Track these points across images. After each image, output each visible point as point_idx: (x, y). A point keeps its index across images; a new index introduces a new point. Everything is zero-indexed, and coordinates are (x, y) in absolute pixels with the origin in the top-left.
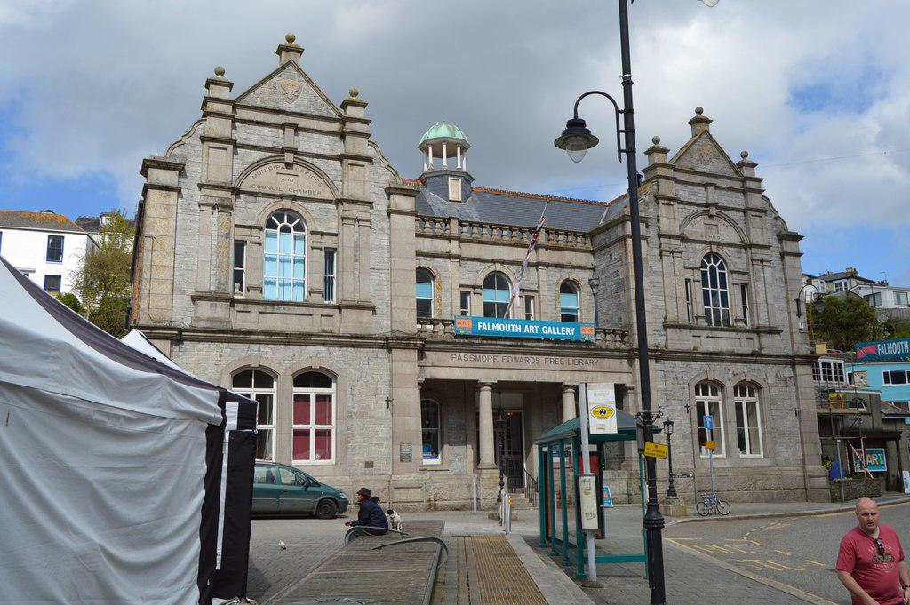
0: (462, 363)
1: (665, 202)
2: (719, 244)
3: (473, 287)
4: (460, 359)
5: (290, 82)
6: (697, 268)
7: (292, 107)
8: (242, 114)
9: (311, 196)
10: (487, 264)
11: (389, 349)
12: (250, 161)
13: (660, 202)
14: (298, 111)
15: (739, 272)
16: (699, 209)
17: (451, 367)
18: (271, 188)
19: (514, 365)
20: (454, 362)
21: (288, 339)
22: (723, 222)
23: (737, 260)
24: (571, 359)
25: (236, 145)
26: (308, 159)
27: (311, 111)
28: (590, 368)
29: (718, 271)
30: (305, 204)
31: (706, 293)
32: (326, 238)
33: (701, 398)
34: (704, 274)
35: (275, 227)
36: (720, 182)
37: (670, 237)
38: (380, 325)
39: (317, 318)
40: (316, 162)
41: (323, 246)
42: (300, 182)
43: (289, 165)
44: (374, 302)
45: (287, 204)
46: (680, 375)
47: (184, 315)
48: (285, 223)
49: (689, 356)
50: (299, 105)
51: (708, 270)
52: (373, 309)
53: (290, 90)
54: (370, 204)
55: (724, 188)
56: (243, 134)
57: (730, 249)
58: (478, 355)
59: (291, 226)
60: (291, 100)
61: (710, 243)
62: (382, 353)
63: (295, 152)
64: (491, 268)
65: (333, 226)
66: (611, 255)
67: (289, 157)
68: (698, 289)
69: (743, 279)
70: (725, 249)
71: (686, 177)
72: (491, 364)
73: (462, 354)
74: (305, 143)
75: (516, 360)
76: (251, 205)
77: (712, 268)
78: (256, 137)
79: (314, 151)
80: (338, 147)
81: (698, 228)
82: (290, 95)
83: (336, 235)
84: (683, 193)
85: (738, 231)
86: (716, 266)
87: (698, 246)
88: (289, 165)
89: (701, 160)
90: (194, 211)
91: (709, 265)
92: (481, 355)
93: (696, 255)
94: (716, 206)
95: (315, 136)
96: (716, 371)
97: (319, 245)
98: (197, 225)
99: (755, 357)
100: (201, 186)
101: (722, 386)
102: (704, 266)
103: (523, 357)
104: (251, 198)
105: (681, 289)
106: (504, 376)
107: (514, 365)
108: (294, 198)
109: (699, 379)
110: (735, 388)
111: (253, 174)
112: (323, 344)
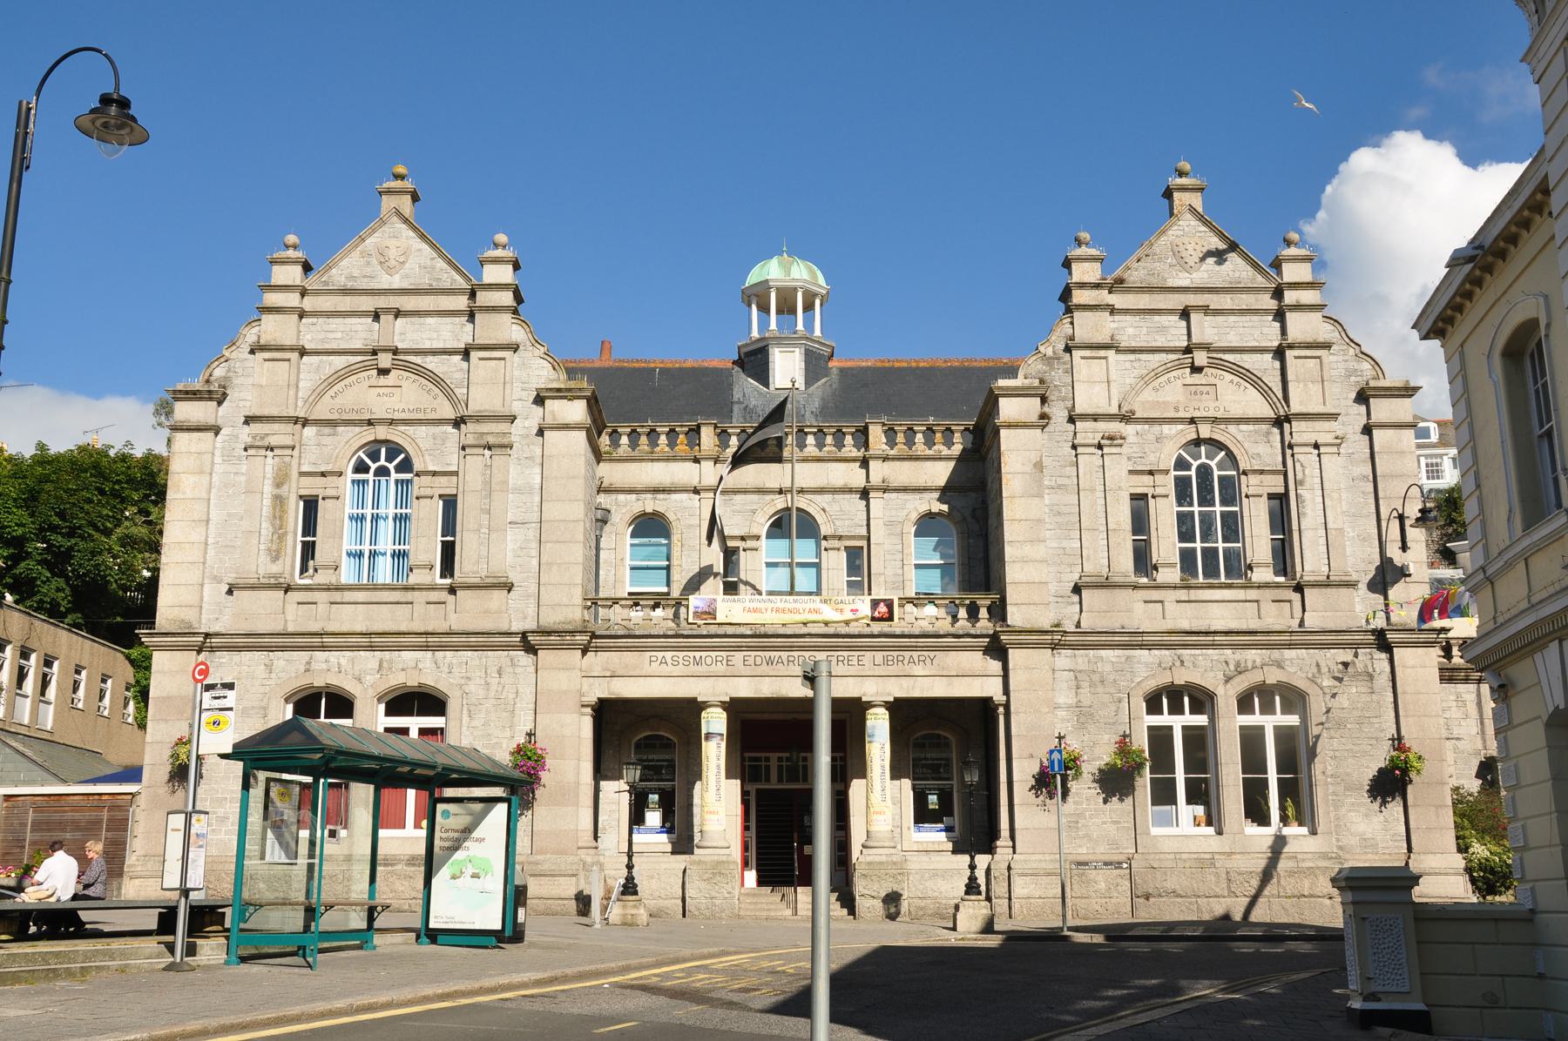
1: (1087, 353)
2: (1215, 421)
3: (743, 538)
4: (664, 662)
5: (392, 243)
6: (1167, 472)
7: (397, 282)
8: (309, 303)
10: (768, 497)
11: (531, 649)
12: (328, 371)
14: (405, 285)
15: (1262, 472)
16: (1163, 357)
17: (651, 678)
18: (418, 410)
19: (764, 669)
21: (373, 641)
22: (1229, 377)
23: (1262, 449)
24: (879, 656)
25: (303, 352)
26: (417, 360)
27: (425, 282)
29: (1216, 473)
30: (410, 430)
31: (1184, 520)
32: (443, 480)
33: (1164, 719)
34: (1182, 487)
35: (366, 470)
37: (1095, 418)
38: (517, 614)
39: (419, 608)
40: (431, 363)
41: (437, 492)
42: (404, 396)
43: (384, 372)
44: (513, 577)
45: (382, 432)
46: (1111, 678)
47: (220, 616)
49: (1135, 641)
50: (407, 276)
51: (1193, 473)
52: (509, 587)
53: (393, 254)
54: (513, 418)
55: (1232, 312)
56: (311, 332)
57: (1243, 427)
58: (698, 654)
59: (391, 466)
60: (390, 271)
61: (1192, 421)
62: (522, 657)
63: (395, 351)
64: (780, 503)
65: (452, 461)
67: (385, 360)
68: (1164, 514)
69: (1275, 484)
70: (1232, 428)
71: (1144, 301)
72: (721, 668)
73: (668, 655)
74: (405, 333)
75: (770, 662)
76: (326, 440)
77: (1204, 472)
78: (339, 335)
79: (427, 345)
80: (461, 333)
81: (1174, 393)
82: (392, 263)
83: (456, 473)
84: (1130, 330)
85: (1265, 391)
87: (1166, 429)
88: (384, 372)
89: (1182, 264)
90: (239, 458)
91: (1195, 464)
92: (704, 654)
93: (1168, 446)
94: (1207, 347)
95: (429, 320)
96: (1202, 668)
97: (428, 492)
98: (243, 478)
99: (1301, 638)
100: (248, 420)
102: (1181, 464)
103: (784, 655)
104: (327, 430)
105: (1122, 515)
106: (745, 689)
107: (764, 669)
108: (392, 422)
111: (331, 392)
112: (426, 648)
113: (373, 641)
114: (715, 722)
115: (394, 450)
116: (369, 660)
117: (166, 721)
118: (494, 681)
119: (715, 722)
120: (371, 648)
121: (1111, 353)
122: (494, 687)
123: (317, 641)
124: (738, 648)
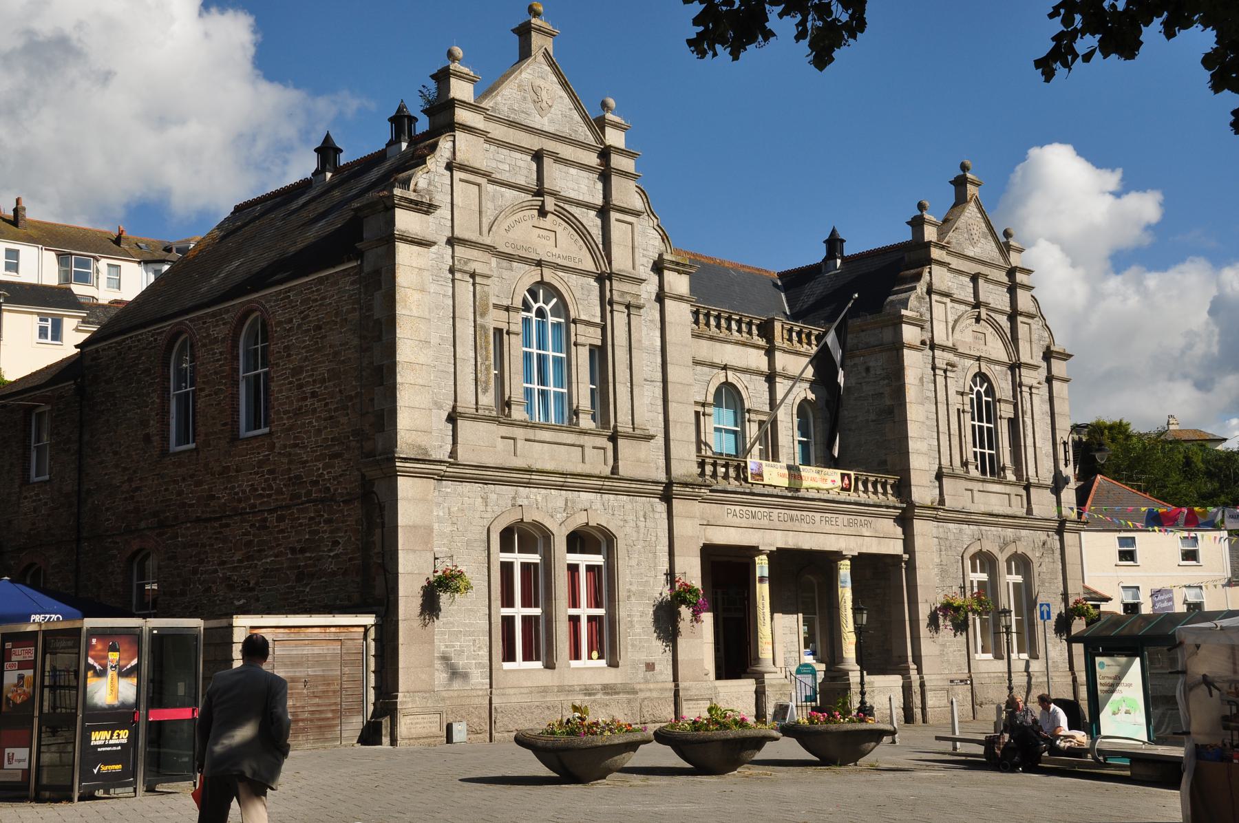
0: (737, 521)
9: (571, 264)
13: (934, 297)
19: (789, 525)
20: (730, 519)
21: (565, 481)
28: (865, 532)
36: (566, 151)
48: (541, 304)
66: (868, 370)
72: (765, 522)
86: (982, 391)
95: (573, 171)
101: (547, 535)
104: (505, 263)
107: (789, 525)
109: (972, 550)
110: (1008, 561)
113: (565, 481)
114: (762, 566)
115: (552, 291)
116: (557, 498)
117: (414, 551)
118: (642, 524)
119: (762, 566)
120: (561, 487)
121: (947, 300)
122: (642, 531)
123: (526, 477)
124: (776, 506)
